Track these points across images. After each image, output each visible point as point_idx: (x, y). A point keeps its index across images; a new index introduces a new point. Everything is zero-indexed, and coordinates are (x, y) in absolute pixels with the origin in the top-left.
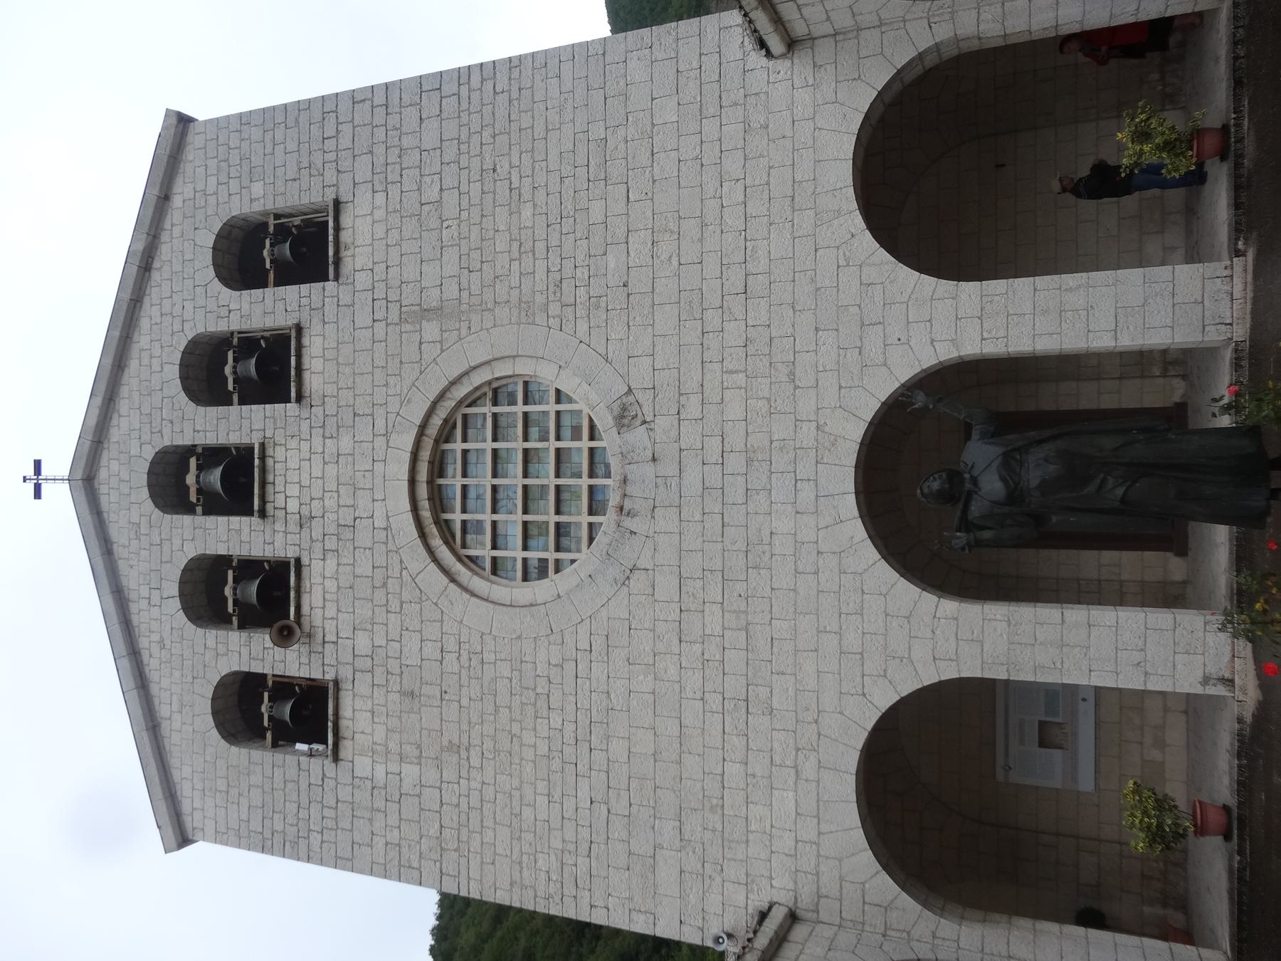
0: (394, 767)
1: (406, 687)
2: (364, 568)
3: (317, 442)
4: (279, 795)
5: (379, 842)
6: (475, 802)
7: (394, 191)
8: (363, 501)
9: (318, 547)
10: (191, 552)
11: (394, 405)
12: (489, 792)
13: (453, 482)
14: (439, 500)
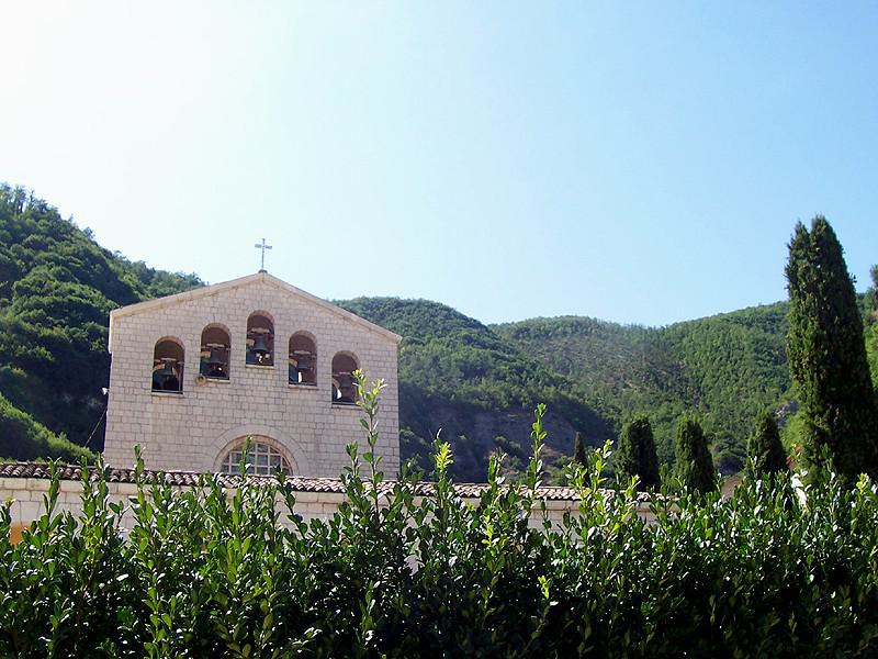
0: (151, 422)
2: (227, 413)
3: (273, 395)
5: (121, 413)
8: (251, 414)
10: (232, 331)
11: (285, 430)
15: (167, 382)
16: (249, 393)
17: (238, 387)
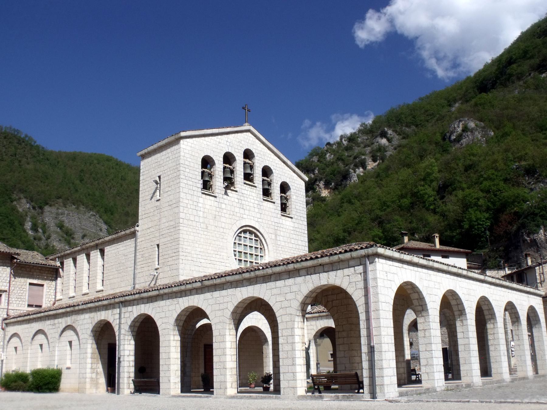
1: (217, 217)
2: (237, 210)
4: (193, 172)
5: (187, 201)
6: (198, 231)
7: (292, 232)
9: (239, 197)
12: (200, 235)
13: (248, 235)
16: (246, 199)
17: (241, 194)
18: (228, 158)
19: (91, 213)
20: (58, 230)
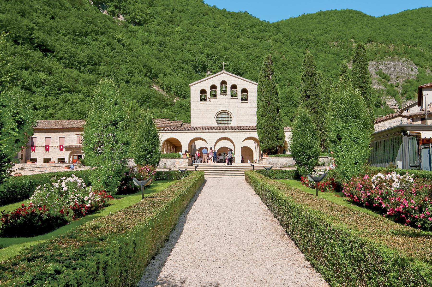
13: (224, 114)
14: (222, 113)
15: (202, 99)
18: (213, 87)
19: (404, 59)
20: (378, 76)
